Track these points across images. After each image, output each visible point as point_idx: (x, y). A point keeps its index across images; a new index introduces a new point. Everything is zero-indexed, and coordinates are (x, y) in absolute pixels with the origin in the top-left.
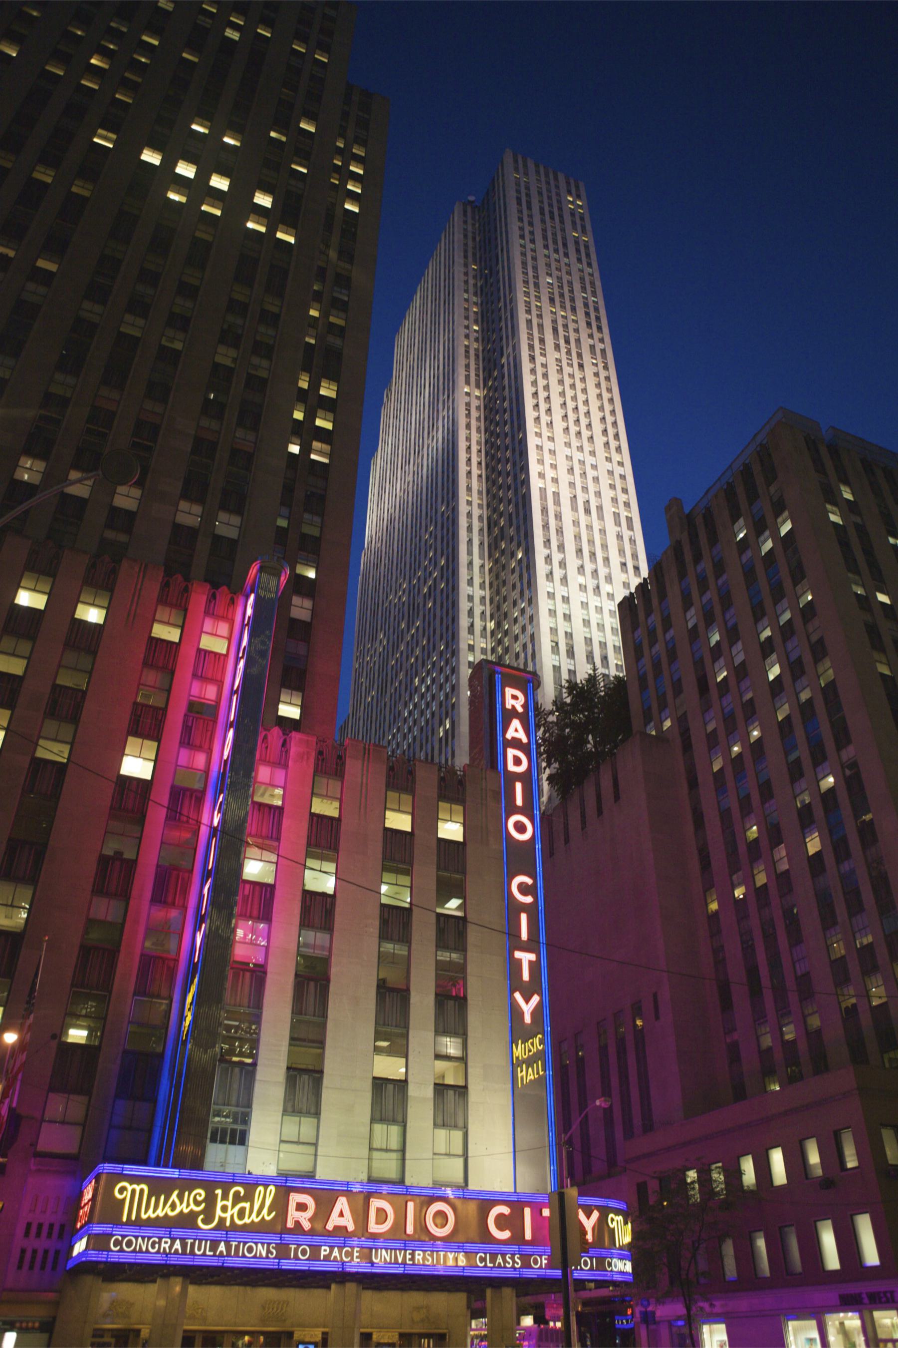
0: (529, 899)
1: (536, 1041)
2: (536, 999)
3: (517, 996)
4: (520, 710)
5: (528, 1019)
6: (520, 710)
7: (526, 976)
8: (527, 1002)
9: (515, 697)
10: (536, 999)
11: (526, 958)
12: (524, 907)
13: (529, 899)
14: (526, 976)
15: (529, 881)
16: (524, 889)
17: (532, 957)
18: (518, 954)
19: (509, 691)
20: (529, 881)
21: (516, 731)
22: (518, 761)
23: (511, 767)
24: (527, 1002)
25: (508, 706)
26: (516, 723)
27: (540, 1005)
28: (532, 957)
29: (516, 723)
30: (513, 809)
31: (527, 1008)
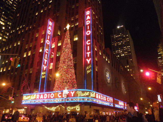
0: (47, 53)
1: (45, 72)
2: (46, 67)
3: (44, 66)
4: (51, 25)
5: (44, 69)
6: (51, 25)
7: (45, 63)
8: (45, 66)
9: (51, 23)
10: (46, 67)
11: (46, 61)
12: (47, 54)
13: (47, 53)
14: (45, 63)
15: (48, 50)
16: (47, 50)
17: (46, 61)
18: (45, 60)
19: (50, 22)
20: (48, 50)
21: (50, 28)
22: (49, 33)
23: (48, 33)
24: (45, 66)
25: (50, 24)
26: (50, 27)
27: (46, 68)
28: (46, 61)
29: (50, 27)
30: (47, 39)
31: (45, 68)
